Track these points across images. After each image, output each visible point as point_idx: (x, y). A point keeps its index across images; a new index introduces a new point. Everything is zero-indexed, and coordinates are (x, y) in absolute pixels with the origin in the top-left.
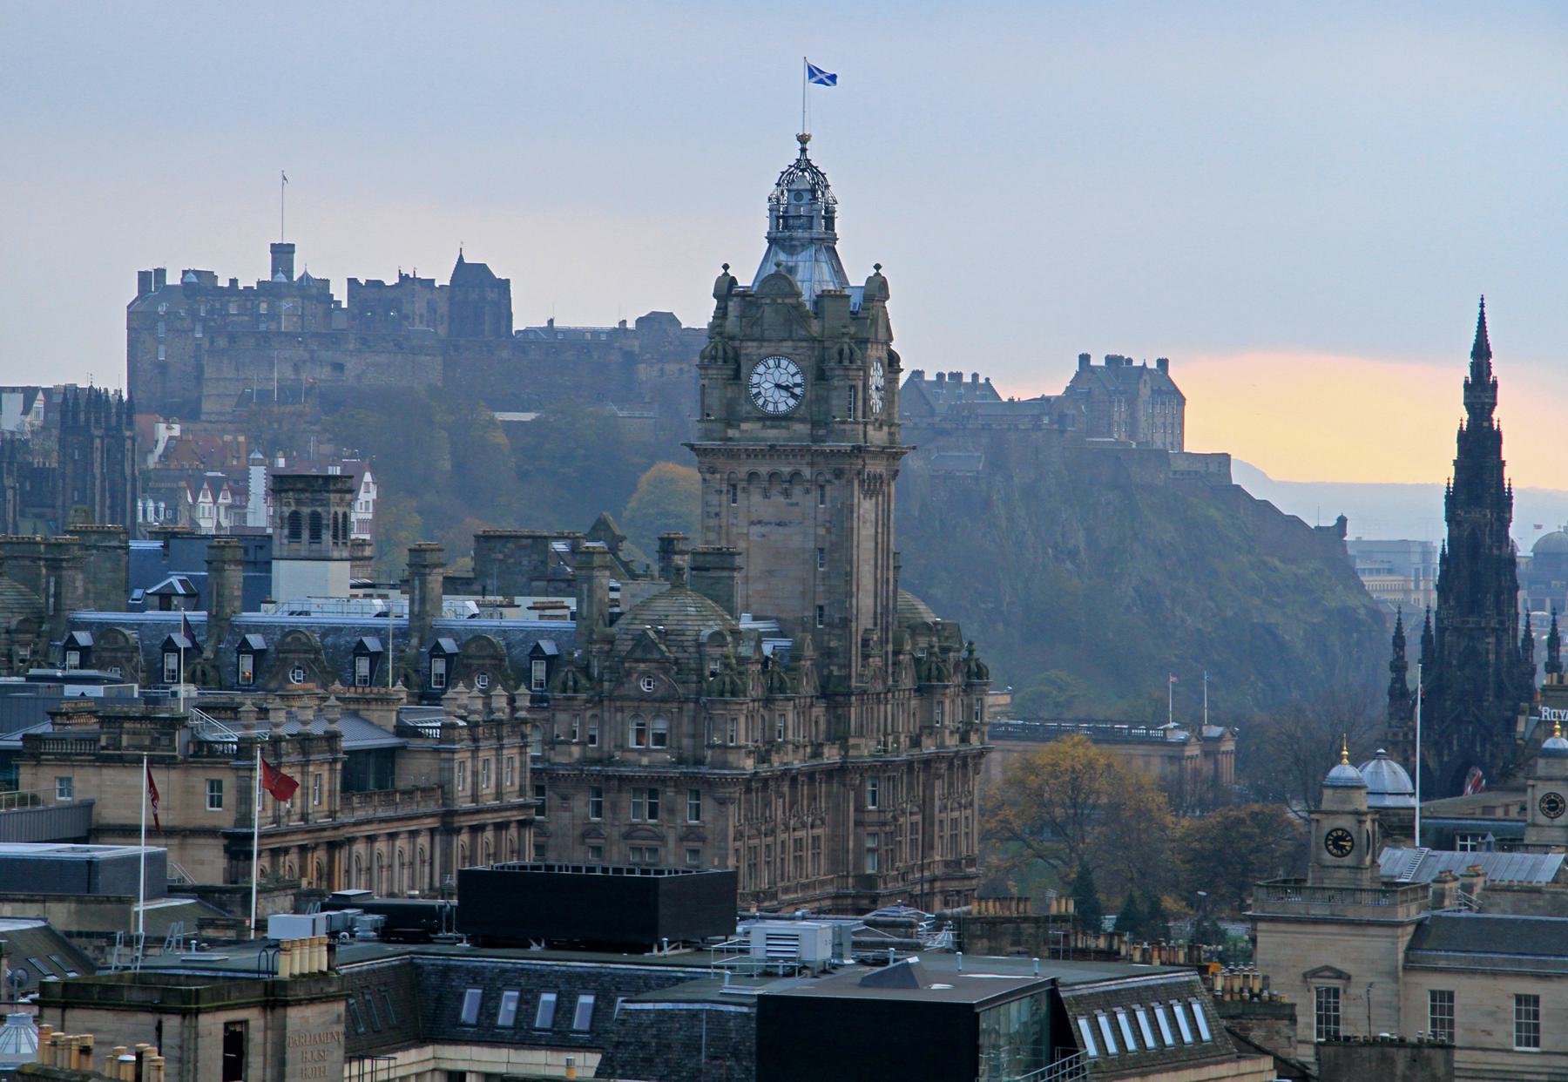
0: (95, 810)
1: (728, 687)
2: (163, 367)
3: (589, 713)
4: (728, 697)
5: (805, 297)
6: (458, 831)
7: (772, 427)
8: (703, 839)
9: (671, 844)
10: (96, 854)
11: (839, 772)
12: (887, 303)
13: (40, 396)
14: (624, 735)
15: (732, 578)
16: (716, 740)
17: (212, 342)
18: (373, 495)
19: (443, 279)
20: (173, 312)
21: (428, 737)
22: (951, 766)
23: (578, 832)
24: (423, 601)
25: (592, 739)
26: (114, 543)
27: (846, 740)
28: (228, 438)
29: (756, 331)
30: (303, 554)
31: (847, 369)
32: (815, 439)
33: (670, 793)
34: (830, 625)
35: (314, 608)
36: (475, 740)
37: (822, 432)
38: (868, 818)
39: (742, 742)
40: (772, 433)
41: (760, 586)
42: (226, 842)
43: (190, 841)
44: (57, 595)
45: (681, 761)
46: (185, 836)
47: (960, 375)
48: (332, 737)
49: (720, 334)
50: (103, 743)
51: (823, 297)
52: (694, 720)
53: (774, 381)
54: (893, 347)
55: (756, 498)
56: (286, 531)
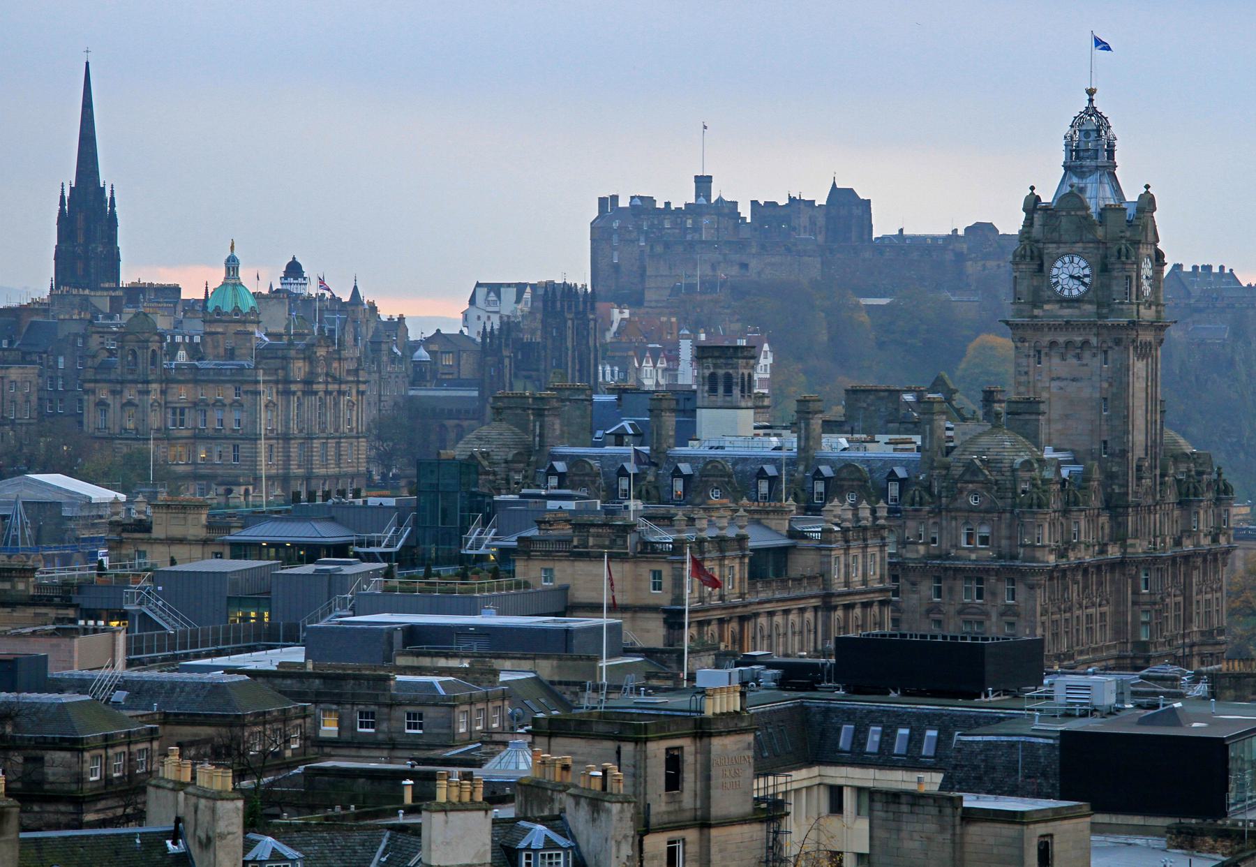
0: (570, 592)
1: (1035, 501)
2: (616, 268)
3: (931, 521)
4: (1035, 509)
5: (1093, 209)
6: (835, 608)
8: (1017, 615)
9: (994, 619)
10: (571, 624)
11: (1120, 565)
13: (528, 289)
14: (957, 537)
16: (1027, 541)
17: (652, 248)
18: (770, 360)
19: (821, 200)
20: (625, 227)
21: (812, 539)
22: (1205, 561)
23: (923, 609)
24: (807, 439)
25: (934, 541)
26: (582, 397)
27: (1125, 541)
28: (664, 319)
29: (1056, 235)
30: (719, 404)
31: (1124, 263)
32: (1100, 316)
33: (993, 580)
34: (1112, 455)
35: (727, 444)
36: (847, 541)
37: (1105, 311)
38: (1142, 599)
39: (1047, 542)
40: (1067, 312)
41: (1059, 426)
42: (662, 616)
43: (640, 615)
44: (541, 435)
45: (1000, 556)
46: (635, 612)
47: (1210, 267)
48: (742, 539)
49: (1028, 238)
50: (575, 543)
51: (1105, 210)
52: (1010, 526)
53: (1069, 273)
54: (1160, 246)
55: (1056, 360)
56: (706, 388)
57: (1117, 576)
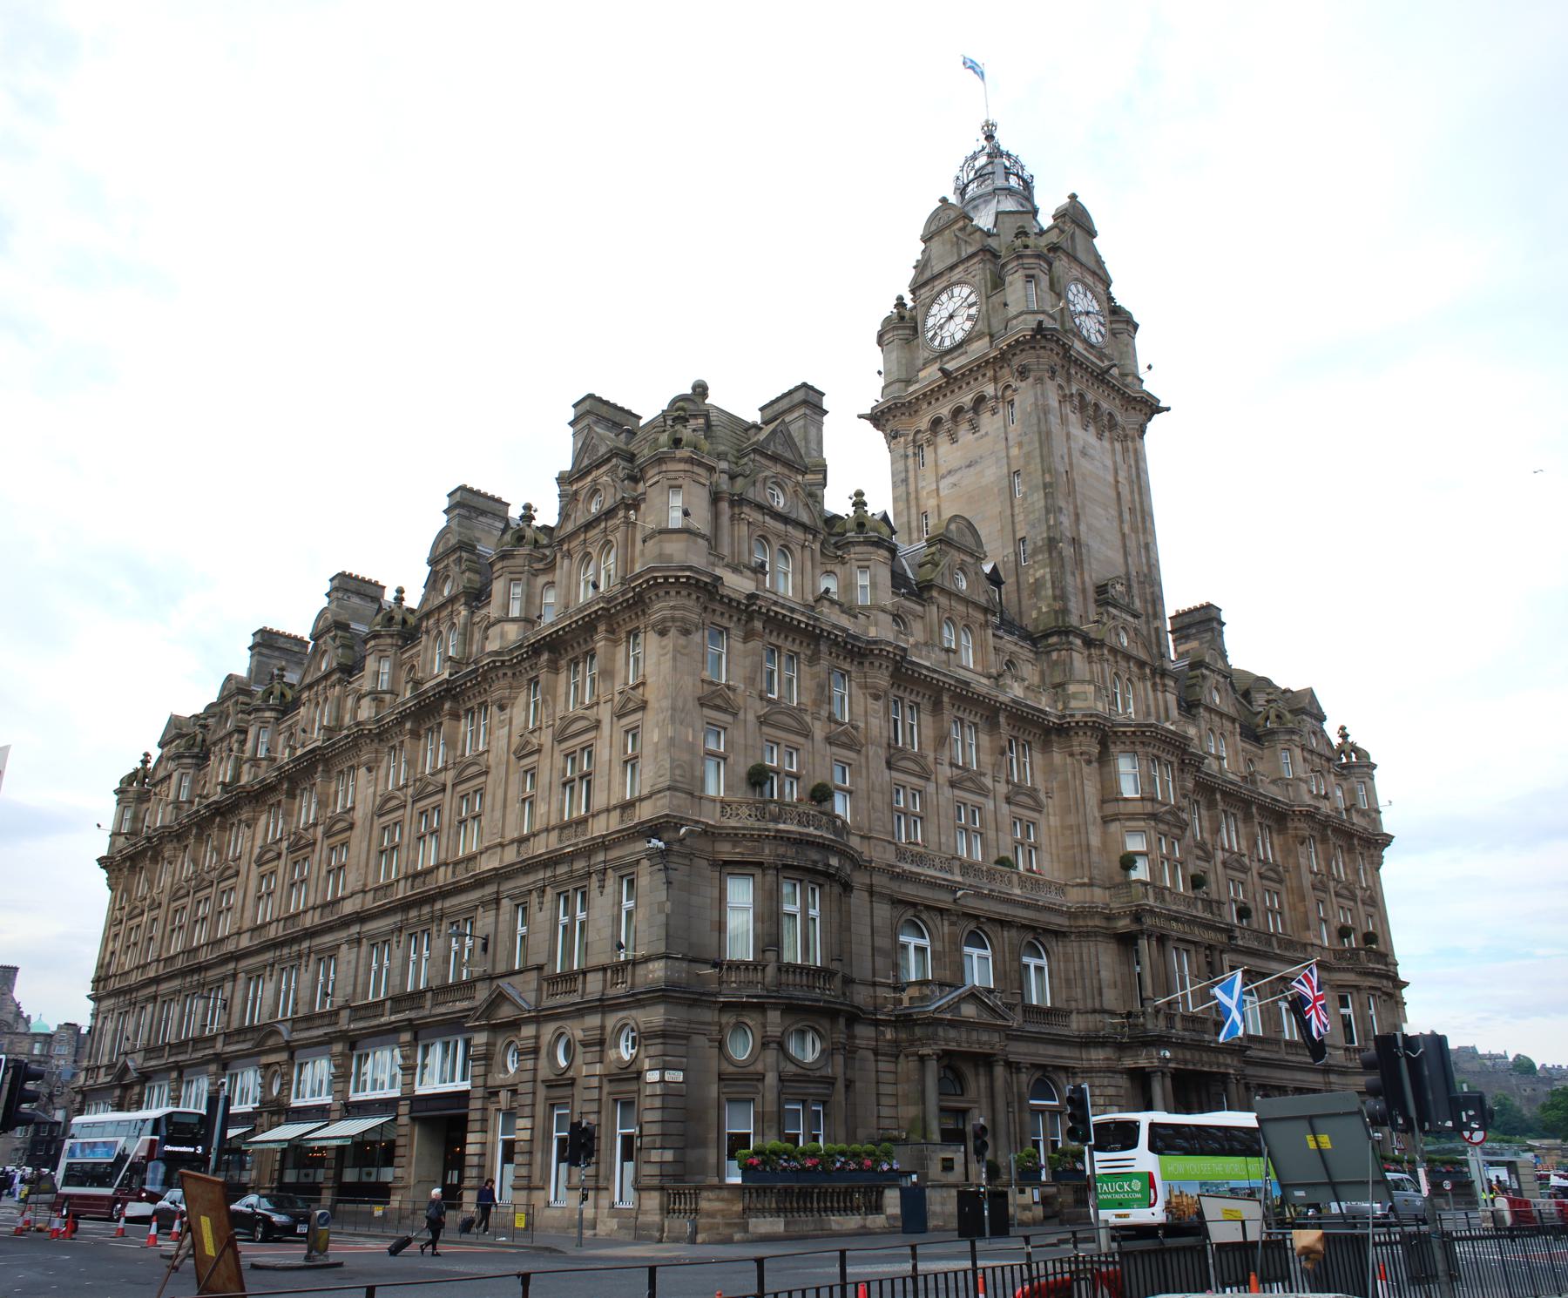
3: (542, 580)
12: (1095, 241)
54: (1122, 295)
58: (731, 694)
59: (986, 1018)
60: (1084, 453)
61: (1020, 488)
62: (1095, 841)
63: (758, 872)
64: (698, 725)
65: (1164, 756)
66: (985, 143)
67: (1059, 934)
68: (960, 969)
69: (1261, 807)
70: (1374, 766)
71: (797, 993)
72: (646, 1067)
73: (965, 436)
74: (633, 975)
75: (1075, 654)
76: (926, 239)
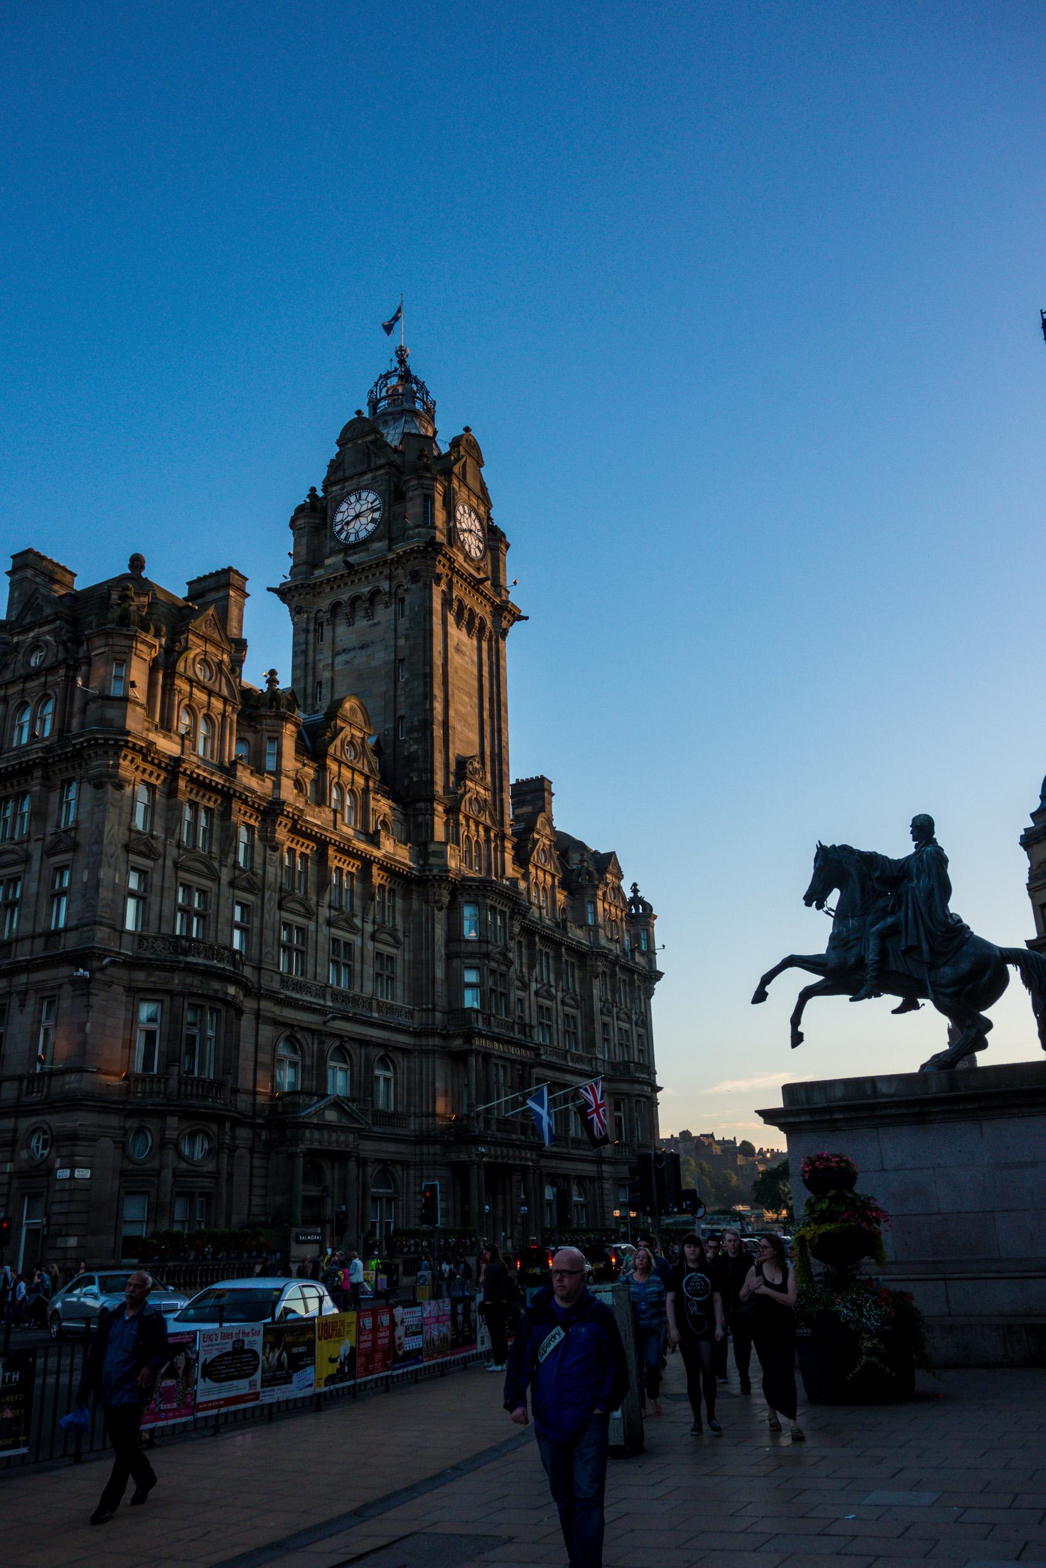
7: (355, 553)
8: (75, 847)
15: (228, 596)
38: (463, 947)
55: (342, 629)
57: (415, 905)
58: (153, 842)
59: (345, 1122)
60: (457, 650)
61: (404, 675)
62: (440, 973)
63: (167, 999)
64: (123, 867)
65: (499, 907)
66: (398, 366)
67: (405, 1051)
68: (322, 1080)
69: (569, 949)
70: (655, 917)
71: (194, 1102)
72: (57, 1165)
73: (362, 623)
74: (49, 1085)
75: (436, 818)
76: (339, 443)
